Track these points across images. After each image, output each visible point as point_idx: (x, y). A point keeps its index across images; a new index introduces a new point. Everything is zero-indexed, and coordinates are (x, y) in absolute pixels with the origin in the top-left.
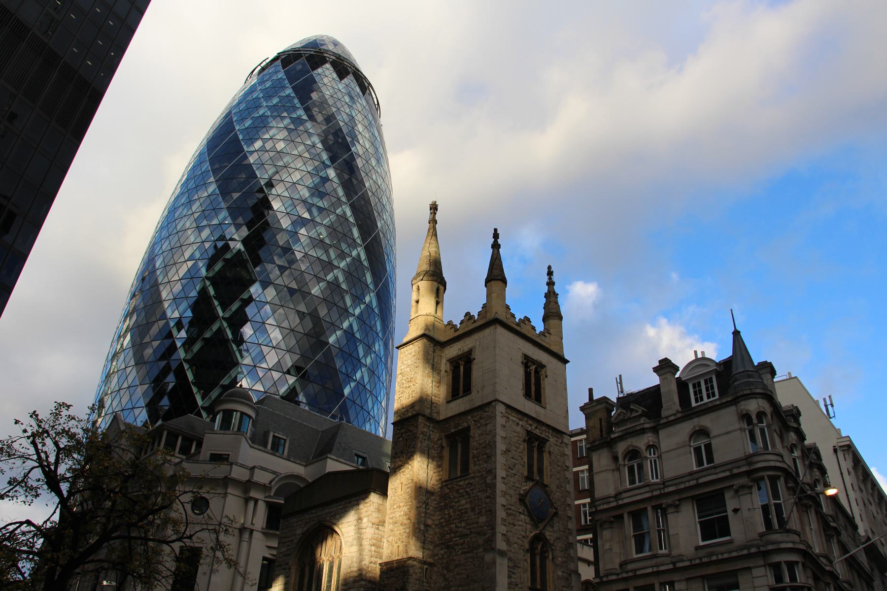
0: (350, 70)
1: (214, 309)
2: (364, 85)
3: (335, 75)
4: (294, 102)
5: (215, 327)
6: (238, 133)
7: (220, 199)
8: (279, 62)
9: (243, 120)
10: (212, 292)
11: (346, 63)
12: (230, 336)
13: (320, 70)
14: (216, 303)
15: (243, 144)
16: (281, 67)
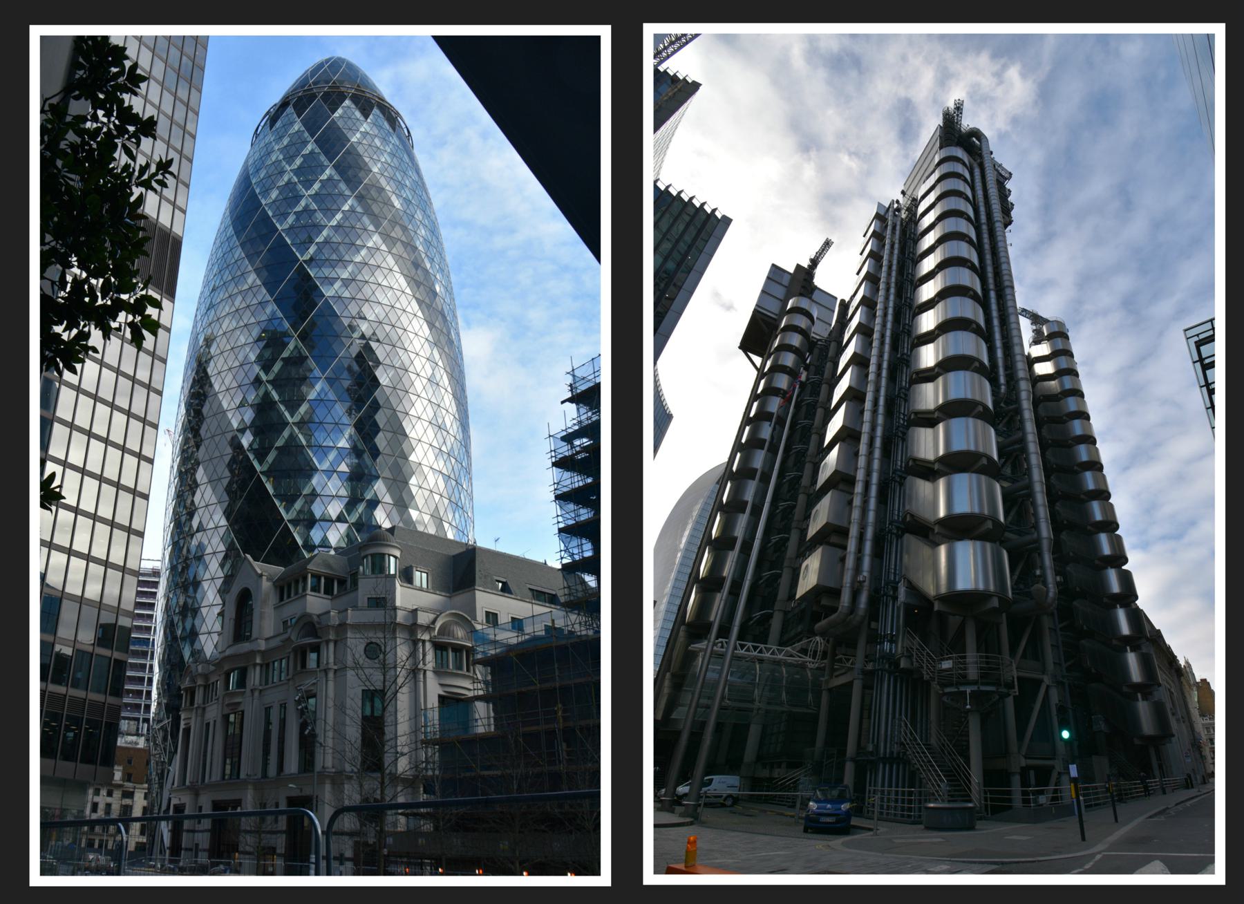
0: (374, 102)
1: (281, 415)
2: (391, 116)
3: (358, 114)
4: (320, 160)
5: (286, 433)
6: (266, 209)
7: (264, 291)
8: (290, 110)
9: (266, 192)
10: (276, 397)
11: (368, 95)
12: (304, 443)
13: (340, 111)
14: (282, 408)
15: (275, 221)
16: (295, 115)
